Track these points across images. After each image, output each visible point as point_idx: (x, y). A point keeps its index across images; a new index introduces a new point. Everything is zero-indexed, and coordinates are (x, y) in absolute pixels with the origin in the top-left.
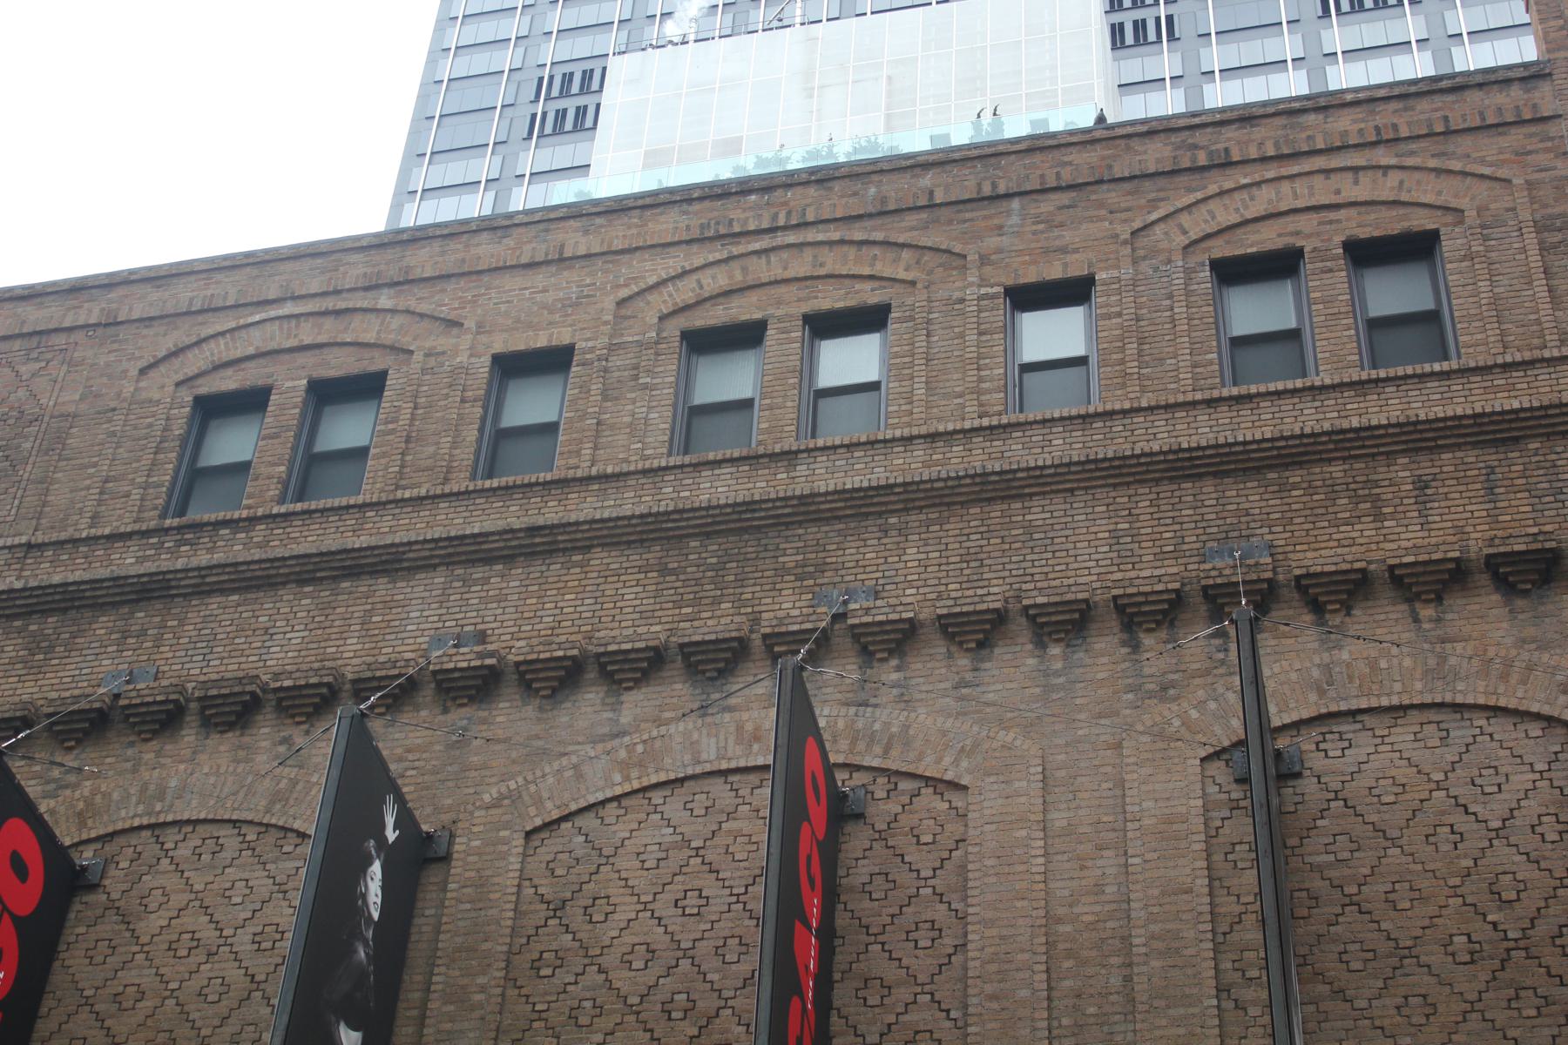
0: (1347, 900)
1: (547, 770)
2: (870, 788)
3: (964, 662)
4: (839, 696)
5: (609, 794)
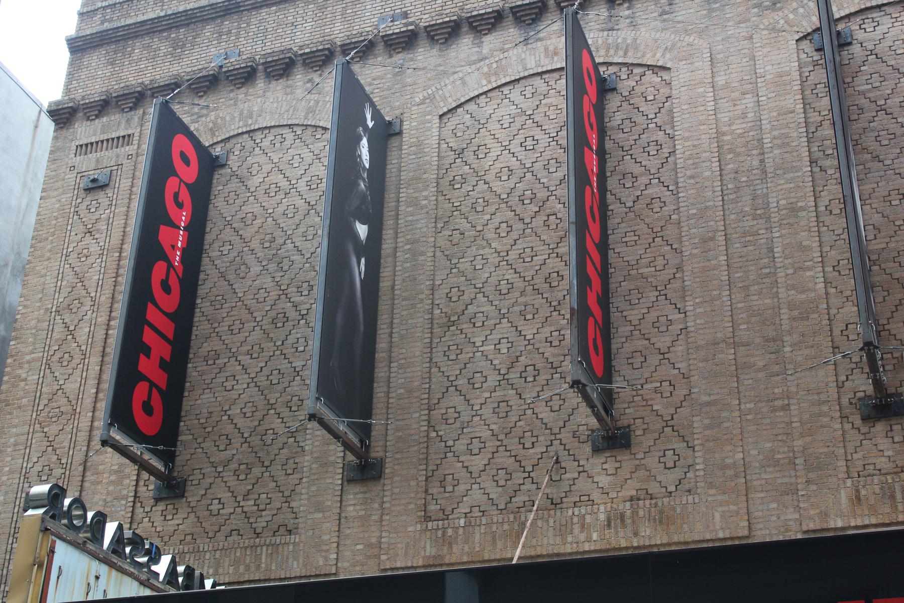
0: (879, 108)
1: (447, 82)
2: (618, 74)
4: (598, 27)
5: (481, 92)
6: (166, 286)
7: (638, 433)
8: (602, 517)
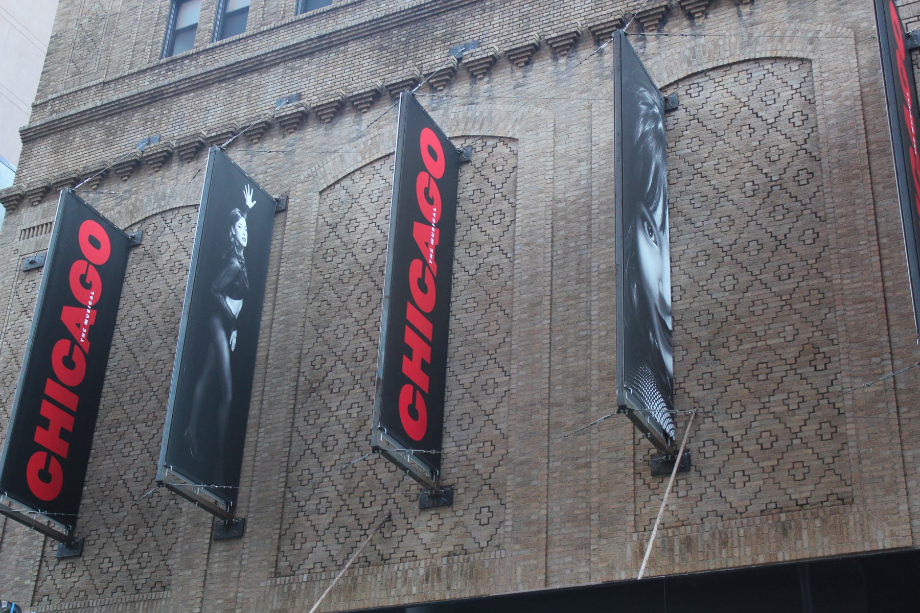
3: (519, 74)
6: (68, 362)
7: (460, 491)
8: (422, 572)
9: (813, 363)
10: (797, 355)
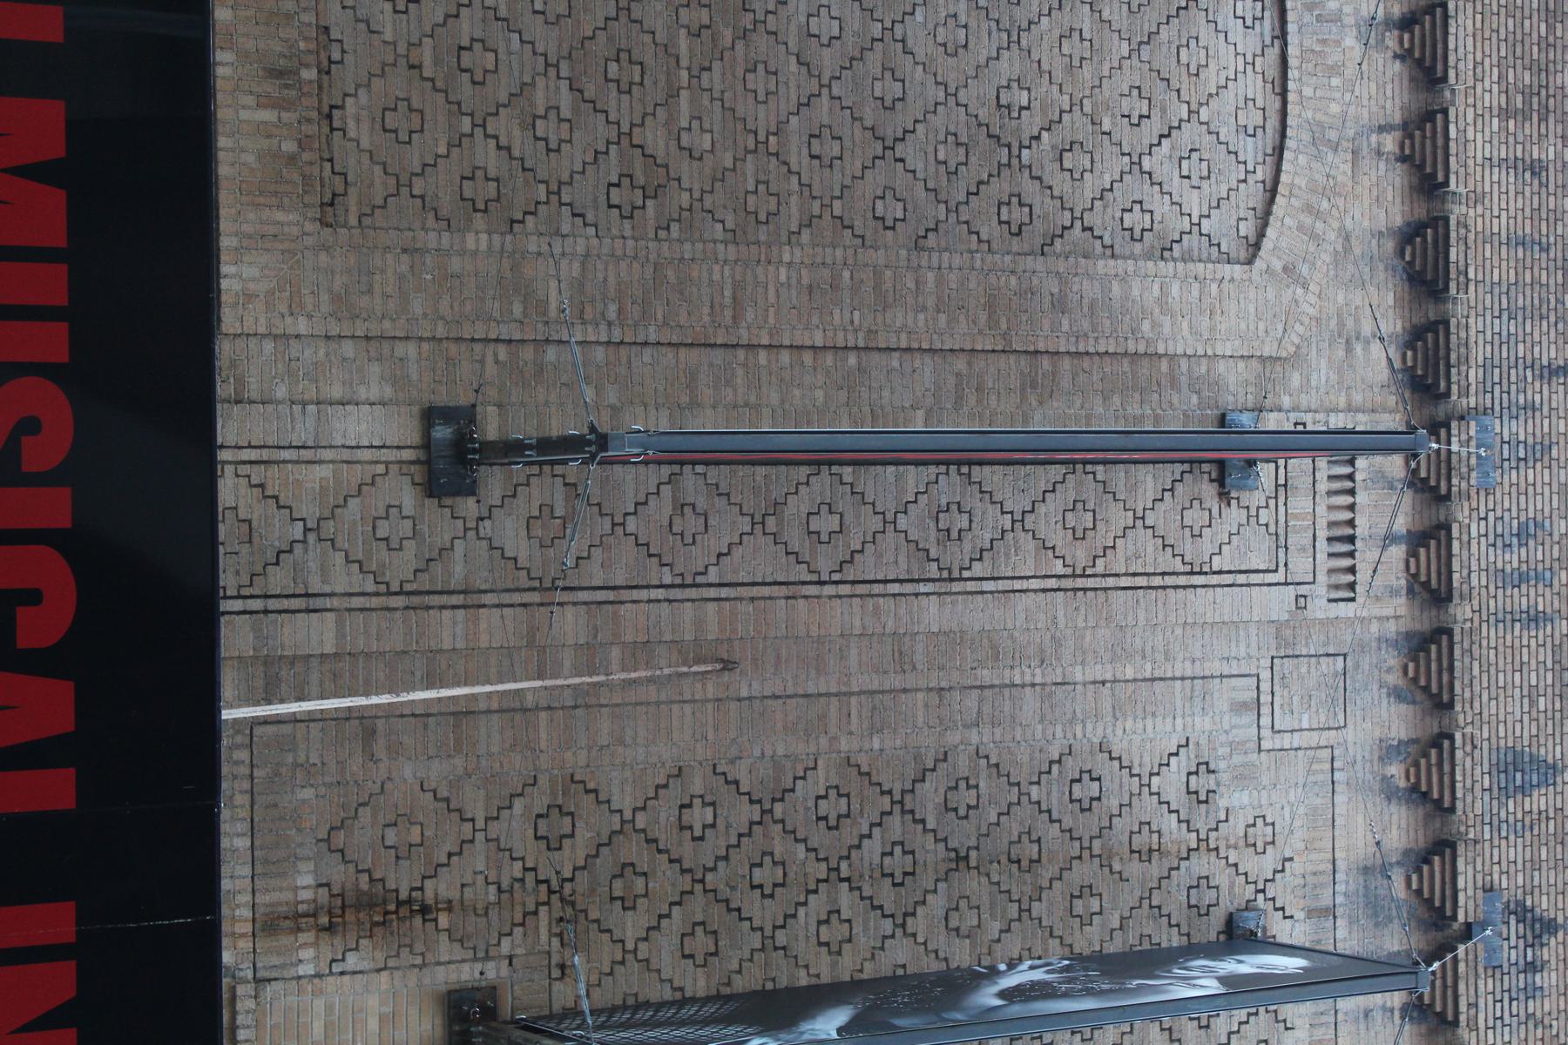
9: (626, 182)
10: (649, 151)
